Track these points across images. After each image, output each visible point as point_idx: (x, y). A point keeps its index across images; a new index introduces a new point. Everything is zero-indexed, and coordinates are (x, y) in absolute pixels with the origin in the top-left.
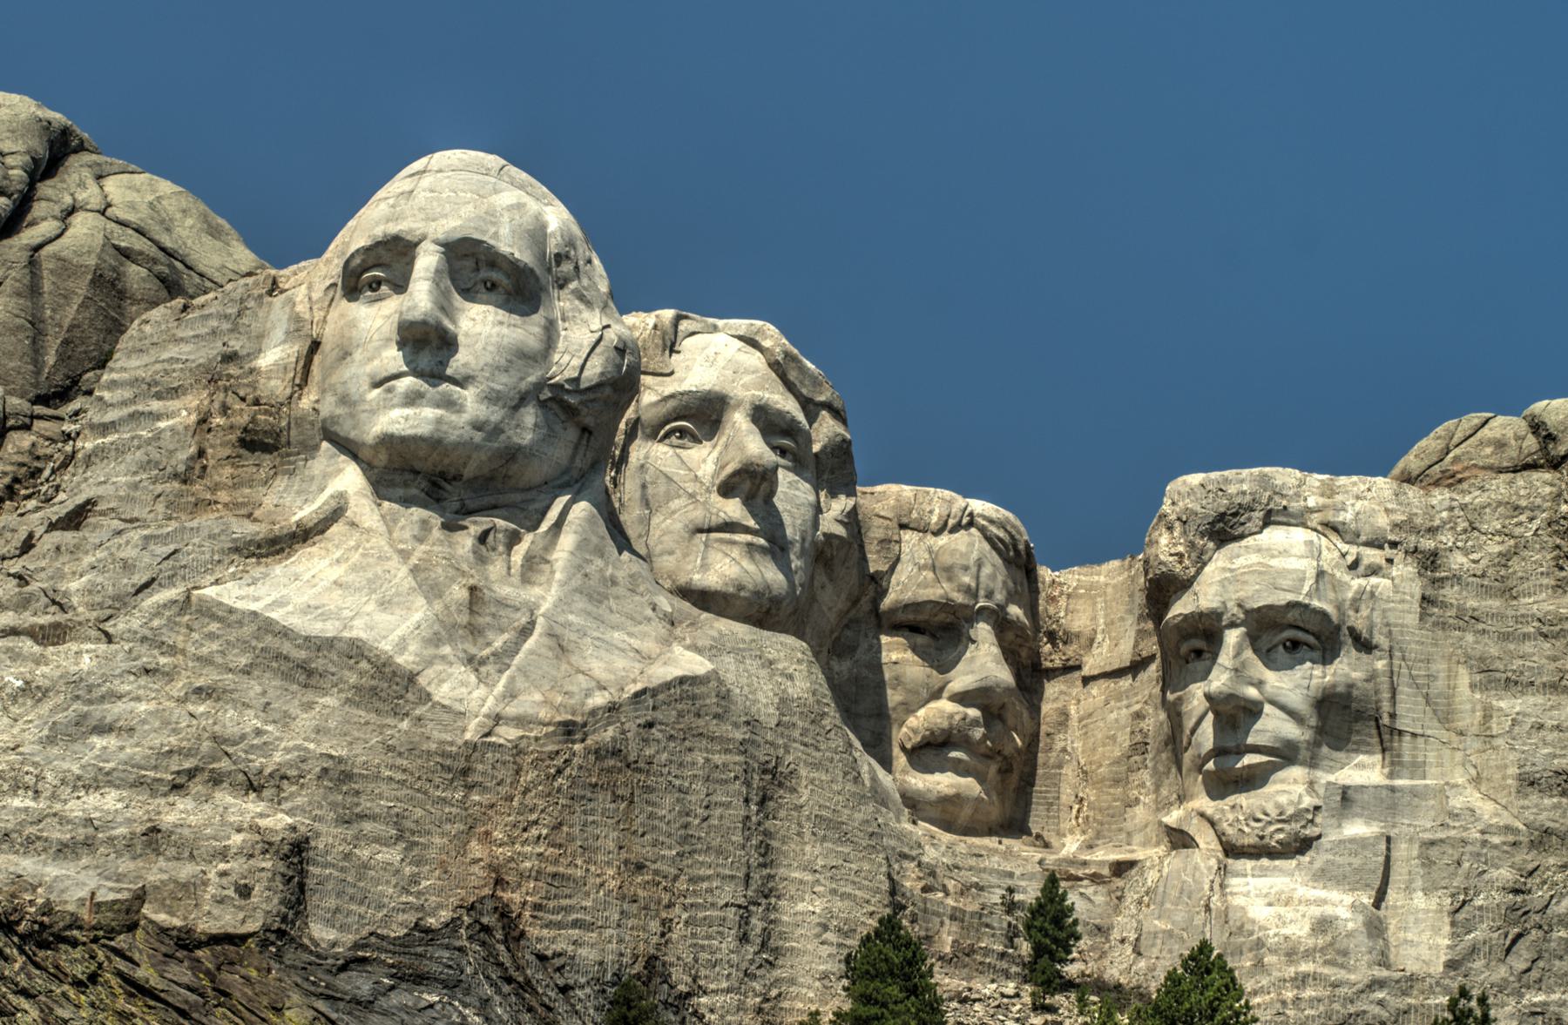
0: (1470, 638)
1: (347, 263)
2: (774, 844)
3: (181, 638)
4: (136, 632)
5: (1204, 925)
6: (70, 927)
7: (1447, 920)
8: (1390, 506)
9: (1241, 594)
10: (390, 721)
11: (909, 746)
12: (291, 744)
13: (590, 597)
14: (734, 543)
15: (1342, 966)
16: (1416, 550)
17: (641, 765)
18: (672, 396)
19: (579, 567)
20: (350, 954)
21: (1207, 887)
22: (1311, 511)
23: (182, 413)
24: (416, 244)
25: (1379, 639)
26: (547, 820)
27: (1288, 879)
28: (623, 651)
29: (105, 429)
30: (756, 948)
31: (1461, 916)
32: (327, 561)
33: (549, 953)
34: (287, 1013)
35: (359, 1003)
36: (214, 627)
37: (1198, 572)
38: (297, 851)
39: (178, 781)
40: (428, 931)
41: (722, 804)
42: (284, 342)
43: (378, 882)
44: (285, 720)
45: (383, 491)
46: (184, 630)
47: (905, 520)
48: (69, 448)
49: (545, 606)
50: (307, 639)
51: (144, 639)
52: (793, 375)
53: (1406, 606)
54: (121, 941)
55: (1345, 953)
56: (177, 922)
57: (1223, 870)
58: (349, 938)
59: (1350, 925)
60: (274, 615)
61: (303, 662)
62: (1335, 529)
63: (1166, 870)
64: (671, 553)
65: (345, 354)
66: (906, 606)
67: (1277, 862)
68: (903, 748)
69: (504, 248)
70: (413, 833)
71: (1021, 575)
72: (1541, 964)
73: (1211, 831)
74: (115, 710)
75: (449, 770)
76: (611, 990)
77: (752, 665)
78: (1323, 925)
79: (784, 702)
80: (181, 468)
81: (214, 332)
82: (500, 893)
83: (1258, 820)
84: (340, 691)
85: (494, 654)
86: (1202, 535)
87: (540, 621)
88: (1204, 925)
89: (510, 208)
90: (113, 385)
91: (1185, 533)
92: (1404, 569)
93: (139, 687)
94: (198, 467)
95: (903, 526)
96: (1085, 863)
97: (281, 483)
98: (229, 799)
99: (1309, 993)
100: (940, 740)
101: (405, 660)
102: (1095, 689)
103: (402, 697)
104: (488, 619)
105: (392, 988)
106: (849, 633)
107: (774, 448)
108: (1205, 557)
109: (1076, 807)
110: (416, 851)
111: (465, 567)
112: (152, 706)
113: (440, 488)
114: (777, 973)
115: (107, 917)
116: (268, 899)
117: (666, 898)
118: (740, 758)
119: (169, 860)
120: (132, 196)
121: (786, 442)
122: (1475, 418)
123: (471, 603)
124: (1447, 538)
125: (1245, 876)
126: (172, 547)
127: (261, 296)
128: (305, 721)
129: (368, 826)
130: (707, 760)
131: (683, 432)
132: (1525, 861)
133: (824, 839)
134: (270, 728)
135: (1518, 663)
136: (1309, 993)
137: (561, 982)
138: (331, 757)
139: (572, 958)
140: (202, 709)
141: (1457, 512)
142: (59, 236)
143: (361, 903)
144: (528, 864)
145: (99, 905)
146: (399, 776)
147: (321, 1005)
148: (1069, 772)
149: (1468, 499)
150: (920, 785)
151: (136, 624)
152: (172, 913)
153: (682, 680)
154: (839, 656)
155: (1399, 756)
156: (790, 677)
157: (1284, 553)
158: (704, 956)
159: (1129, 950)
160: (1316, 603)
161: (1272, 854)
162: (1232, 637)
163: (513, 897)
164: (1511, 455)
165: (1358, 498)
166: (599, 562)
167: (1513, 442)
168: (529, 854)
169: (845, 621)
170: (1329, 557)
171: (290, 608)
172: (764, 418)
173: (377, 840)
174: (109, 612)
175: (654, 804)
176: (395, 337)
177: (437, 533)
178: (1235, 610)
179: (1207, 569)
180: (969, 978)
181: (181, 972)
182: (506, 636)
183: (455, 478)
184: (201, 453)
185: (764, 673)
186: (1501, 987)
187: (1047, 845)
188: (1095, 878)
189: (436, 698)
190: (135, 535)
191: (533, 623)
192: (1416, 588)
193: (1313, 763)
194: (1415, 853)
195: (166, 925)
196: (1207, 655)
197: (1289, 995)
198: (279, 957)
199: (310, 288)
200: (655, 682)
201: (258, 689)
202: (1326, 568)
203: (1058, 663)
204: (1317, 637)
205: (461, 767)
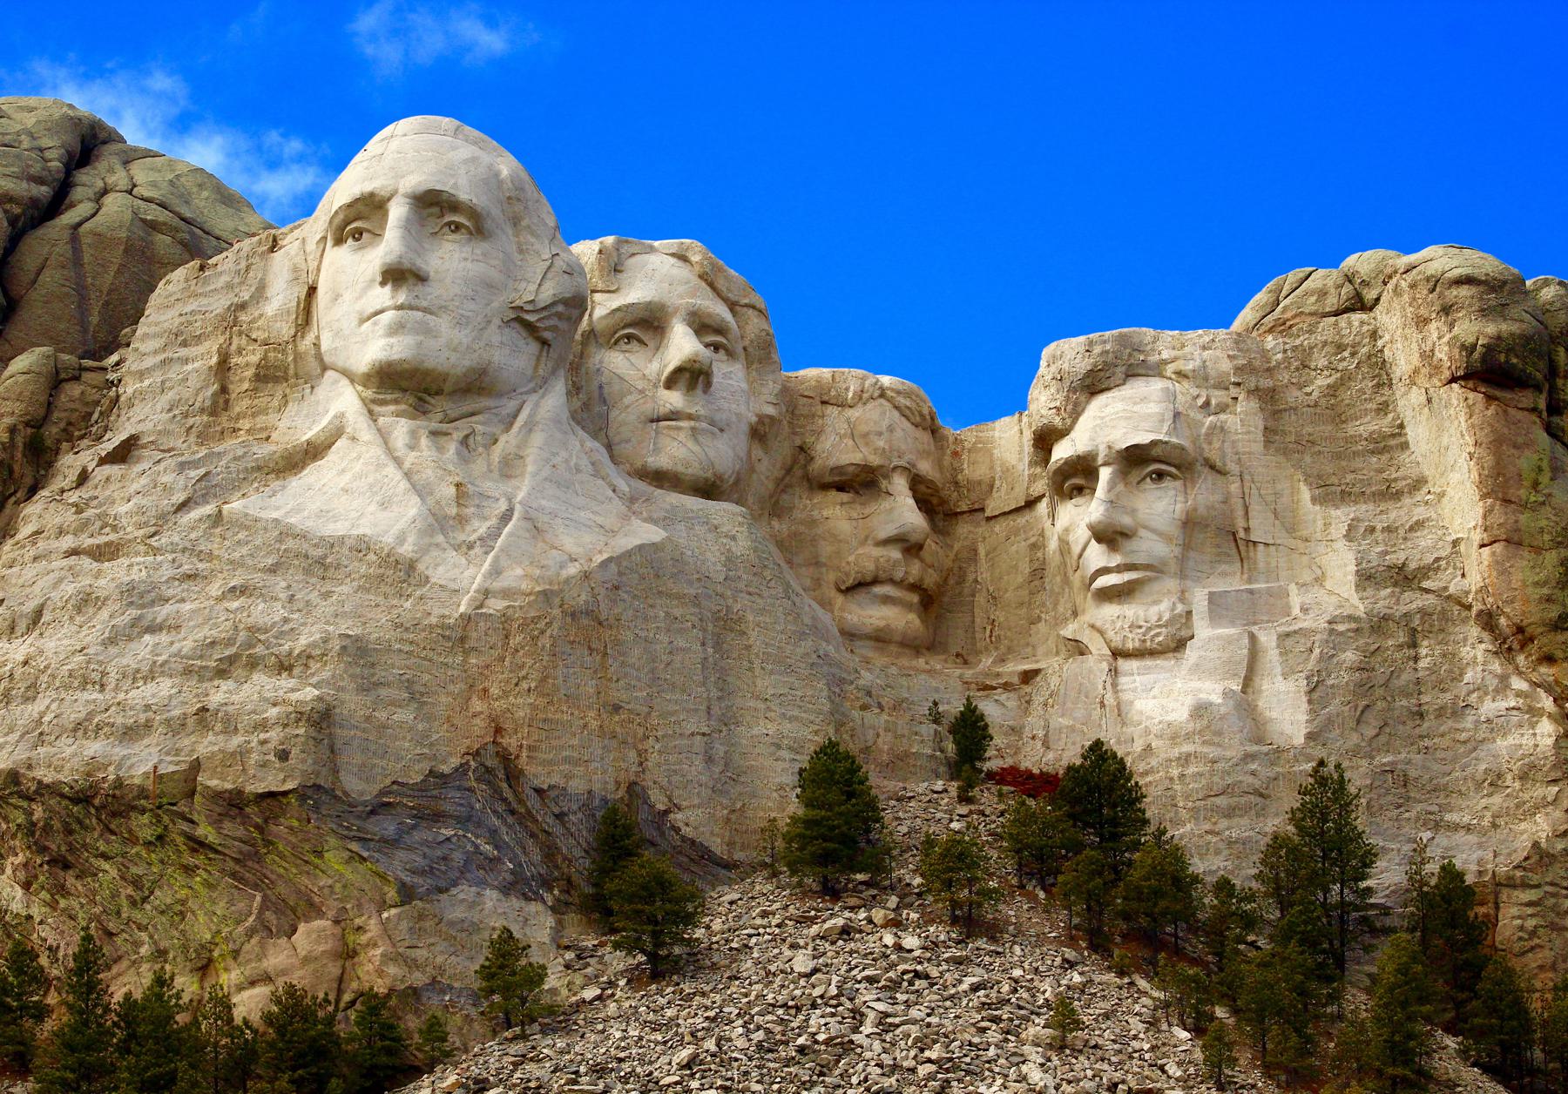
0: (1308, 459)
2: (730, 679)
6: (138, 797)
7: (1305, 699)
9: (1111, 438)
13: (559, 485)
14: (679, 428)
15: (1219, 745)
16: (1257, 389)
17: (612, 620)
18: (618, 309)
19: (547, 461)
20: (375, 801)
22: (1165, 362)
23: (205, 355)
24: (389, 199)
25: (1233, 467)
26: (535, 675)
29: (141, 375)
30: (721, 768)
31: (1315, 696)
33: (545, 787)
34: (326, 855)
35: (383, 840)
38: (321, 719)
40: (443, 776)
41: (683, 649)
43: (396, 738)
45: (377, 409)
47: (825, 398)
48: (112, 393)
49: (520, 496)
50: (322, 538)
51: (184, 550)
53: (1252, 436)
54: (182, 807)
55: (1219, 733)
56: (228, 786)
57: (1114, 672)
58: (375, 788)
59: (1223, 710)
60: (292, 520)
61: (318, 560)
65: (337, 297)
69: (463, 196)
70: (422, 694)
71: (925, 437)
72: (1387, 730)
74: (163, 612)
75: (449, 638)
76: (599, 814)
77: (700, 530)
78: (1200, 710)
80: (208, 403)
82: (499, 740)
87: (518, 508)
89: (466, 162)
90: (146, 335)
95: (823, 403)
96: (998, 675)
97: (292, 407)
99: (1192, 770)
100: (869, 579)
101: (407, 550)
105: (414, 827)
106: (785, 497)
107: (707, 346)
110: (426, 709)
114: (739, 788)
115: (171, 788)
116: (304, 761)
117: (640, 731)
118: (693, 610)
119: (217, 734)
120: (153, 176)
121: (719, 339)
122: (1300, 273)
124: (1284, 377)
126: (202, 471)
129: (383, 692)
130: (667, 614)
131: (629, 337)
132: (1367, 644)
133: (772, 673)
134: (295, 616)
135: (1350, 477)
136: (1192, 770)
137: (557, 810)
138: (349, 636)
139: (564, 789)
140: (236, 604)
142: (93, 215)
143: (382, 758)
144: (522, 714)
145: (161, 776)
146: (407, 648)
147: (354, 846)
148: (980, 599)
149: (1298, 342)
150: (855, 619)
151: (176, 539)
152: (224, 780)
153: (641, 547)
154: (779, 517)
156: (734, 538)
158: (675, 779)
159: (1039, 744)
160: (1174, 440)
161: (1152, 653)
162: (1105, 474)
163: (510, 742)
164: (1332, 302)
166: (564, 454)
167: (1333, 290)
168: (521, 706)
172: (702, 326)
173: (393, 703)
174: (153, 529)
175: (624, 654)
176: (379, 279)
177: (424, 441)
180: (905, 780)
181: (232, 828)
182: (488, 524)
183: (437, 394)
184: (224, 390)
185: (710, 536)
186: (1355, 753)
187: (966, 662)
188: (1007, 687)
190: (170, 462)
191: (511, 510)
192: (1259, 422)
194: (1274, 644)
195: (219, 788)
197: (1175, 772)
198: (316, 808)
200: (618, 551)
201: (283, 584)
203: (965, 508)
204: (1178, 467)
205: (459, 636)
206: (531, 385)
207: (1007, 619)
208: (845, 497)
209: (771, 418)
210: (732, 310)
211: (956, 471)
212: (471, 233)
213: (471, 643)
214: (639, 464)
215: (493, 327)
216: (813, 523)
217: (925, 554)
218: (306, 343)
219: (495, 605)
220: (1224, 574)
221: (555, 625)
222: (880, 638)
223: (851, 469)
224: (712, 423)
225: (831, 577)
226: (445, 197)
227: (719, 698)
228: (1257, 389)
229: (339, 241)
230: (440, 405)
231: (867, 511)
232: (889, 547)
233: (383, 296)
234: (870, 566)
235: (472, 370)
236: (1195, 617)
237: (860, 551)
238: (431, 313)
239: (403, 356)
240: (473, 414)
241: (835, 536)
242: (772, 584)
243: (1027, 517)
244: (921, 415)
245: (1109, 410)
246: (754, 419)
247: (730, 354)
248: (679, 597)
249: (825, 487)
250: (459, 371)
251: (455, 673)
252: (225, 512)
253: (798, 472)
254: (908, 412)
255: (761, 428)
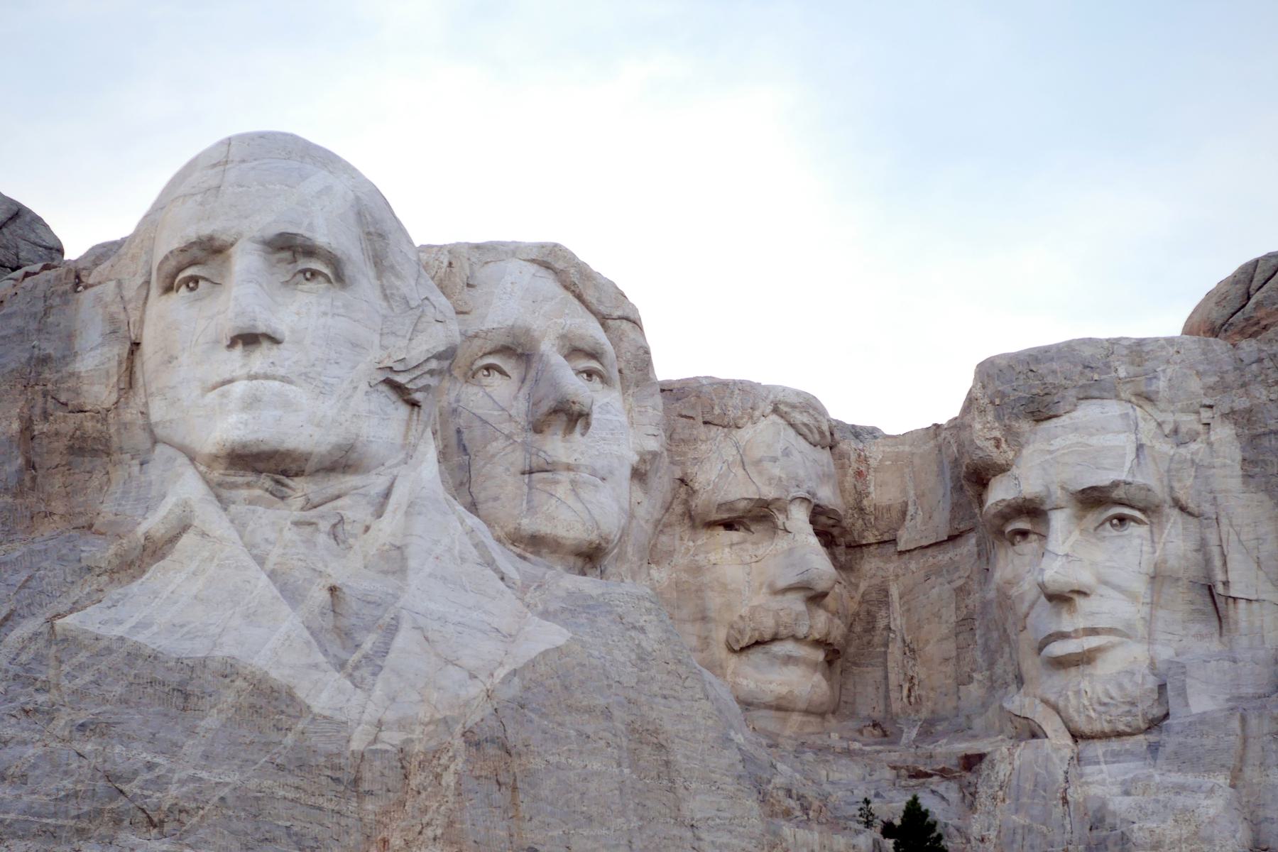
1: (162, 263)
3: (52, 672)
4: (7, 671)
5: (1064, 817)
8: (1201, 368)
10: (275, 736)
11: (737, 648)
12: (183, 775)
16: (1233, 412)
17: (520, 746)
18: (476, 336)
21: (1061, 778)
24: (232, 245)
25: (1207, 508)
26: (440, 820)
27: (1140, 764)
28: (484, 632)
32: (184, 576)
36: (82, 657)
37: (1018, 454)
39: (80, 825)
41: (597, 773)
42: (102, 345)
44: (173, 750)
45: (225, 493)
46: (53, 663)
47: (708, 418)
50: (179, 661)
51: (16, 677)
52: (590, 296)
59: (1212, 812)
60: (141, 638)
62: (1149, 399)
63: (1017, 763)
64: (496, 499)
65: (171, 359)
66: (720, 505)
67: (1129, 743)
68: (732, 651)
69: (321, 238)
71: (825, 456)
73: (1057, 718)
79: (643, 658)
80: (12, 483)
81: (20, 332)
83: (1105, 704)
84: (220, 711)
85: (365, 657)
86: (1017, 417)
88: (1064, 817)
91: (998, 418)
92: (1224, 433)
93: (23, 730)
94: (27, 478)
95: (705, 423)
98: (134, 839)
100: (767, 637)
101: (278, 675)
102: (915, 564)
103: (282, 712)
104: (353, 620)
106: (664, 538)
107: (579, 372)
108: (1022, 440)
109: (906, 687)
111: (320, 566)
112: (39, 750)
113: (283, 485)
121: (594, 364)
123: (333, 605)
125: (1098, 763)
126: (23, 576)
127: (65, 293)
128: (193, 748)
130: (580, 733)
138: (227, 784)
140: (89, 747)
141: (1267, 363)
146: (291, 795)
148: (895, 650)
150: (752, 685)
153: (545, 654)
154: (657, 563)
155: (1236, 623)
157: (1103, 430)
160: (1139, 480)
161: (1119, 734)
162: (1059, 521)
165: (1168, 362)
169: (660, 527)
170: (1147, 430)
171: (155, 628)
177: (290, 534)
178: (1059, 492)
179: (1025, 452)
183: (297, 475)
184: (31, 465)
187: (885, 735)
188: (944, 773)
189: (316, 710)
191: (396, 618)
193: (1150, 639)
196: (1032, 537)
199: (120, 284)
200: (520, 663)
202: (1144, 440)
203: (872, 540)
204: (1140, 510)
206: (402, 456)
207: (929, 676)
208: (734, 536)
209: (655, 455)
210: (603, 325)
211: (861, 495)
212: (329, 281)
213: (365, 786)
214: (510, 527)
215: (360, 394)
216: (697, 570)
217: (828, 600)
218: (131, 414)
219: (392, 738)
220: (1199, 636)
221: (460, 760)
222: (781, 707)
223: (742, 505)
224: (594, 473)
225: (721, 634)
226: (299, 241)
227: (640, 828)
228: (1233, 412)
229: (169, 289)
230: (301, 487)
231: (760, 552)
232: (791, 596)
233: (235, 360)
234: (767, 625)
235: (339, 447)
236: (1170, 693)
237: (755, 602)
238: (290, 382)
239: (261, 436)
240: (338, 497)
241: (724, 587)
242: (687, 683)
243: (951, 554)
244: (822, 433)
245: (1057, 443)
246: (635, 458)
247: (604, 380)
248: (589, 710)
249: (711, 525)
250: (323, 449)
251: (350, 822)
252: (57, 628)
253: (678, 508)
254: (805, 431)
255: (643, 468)
